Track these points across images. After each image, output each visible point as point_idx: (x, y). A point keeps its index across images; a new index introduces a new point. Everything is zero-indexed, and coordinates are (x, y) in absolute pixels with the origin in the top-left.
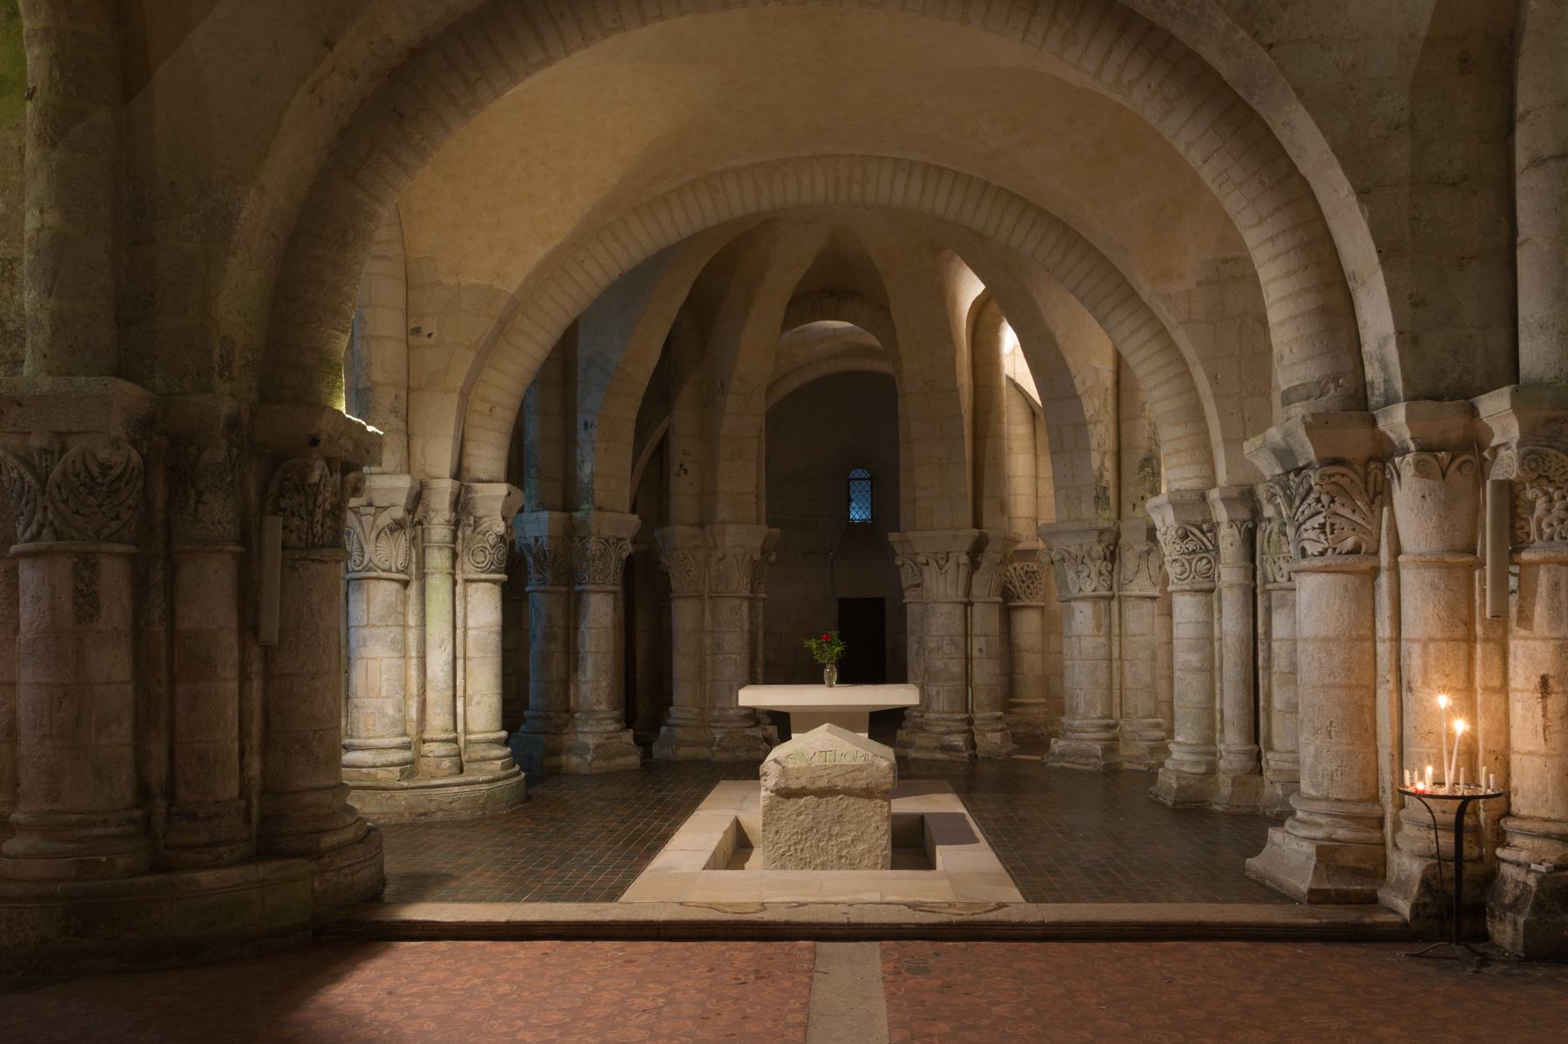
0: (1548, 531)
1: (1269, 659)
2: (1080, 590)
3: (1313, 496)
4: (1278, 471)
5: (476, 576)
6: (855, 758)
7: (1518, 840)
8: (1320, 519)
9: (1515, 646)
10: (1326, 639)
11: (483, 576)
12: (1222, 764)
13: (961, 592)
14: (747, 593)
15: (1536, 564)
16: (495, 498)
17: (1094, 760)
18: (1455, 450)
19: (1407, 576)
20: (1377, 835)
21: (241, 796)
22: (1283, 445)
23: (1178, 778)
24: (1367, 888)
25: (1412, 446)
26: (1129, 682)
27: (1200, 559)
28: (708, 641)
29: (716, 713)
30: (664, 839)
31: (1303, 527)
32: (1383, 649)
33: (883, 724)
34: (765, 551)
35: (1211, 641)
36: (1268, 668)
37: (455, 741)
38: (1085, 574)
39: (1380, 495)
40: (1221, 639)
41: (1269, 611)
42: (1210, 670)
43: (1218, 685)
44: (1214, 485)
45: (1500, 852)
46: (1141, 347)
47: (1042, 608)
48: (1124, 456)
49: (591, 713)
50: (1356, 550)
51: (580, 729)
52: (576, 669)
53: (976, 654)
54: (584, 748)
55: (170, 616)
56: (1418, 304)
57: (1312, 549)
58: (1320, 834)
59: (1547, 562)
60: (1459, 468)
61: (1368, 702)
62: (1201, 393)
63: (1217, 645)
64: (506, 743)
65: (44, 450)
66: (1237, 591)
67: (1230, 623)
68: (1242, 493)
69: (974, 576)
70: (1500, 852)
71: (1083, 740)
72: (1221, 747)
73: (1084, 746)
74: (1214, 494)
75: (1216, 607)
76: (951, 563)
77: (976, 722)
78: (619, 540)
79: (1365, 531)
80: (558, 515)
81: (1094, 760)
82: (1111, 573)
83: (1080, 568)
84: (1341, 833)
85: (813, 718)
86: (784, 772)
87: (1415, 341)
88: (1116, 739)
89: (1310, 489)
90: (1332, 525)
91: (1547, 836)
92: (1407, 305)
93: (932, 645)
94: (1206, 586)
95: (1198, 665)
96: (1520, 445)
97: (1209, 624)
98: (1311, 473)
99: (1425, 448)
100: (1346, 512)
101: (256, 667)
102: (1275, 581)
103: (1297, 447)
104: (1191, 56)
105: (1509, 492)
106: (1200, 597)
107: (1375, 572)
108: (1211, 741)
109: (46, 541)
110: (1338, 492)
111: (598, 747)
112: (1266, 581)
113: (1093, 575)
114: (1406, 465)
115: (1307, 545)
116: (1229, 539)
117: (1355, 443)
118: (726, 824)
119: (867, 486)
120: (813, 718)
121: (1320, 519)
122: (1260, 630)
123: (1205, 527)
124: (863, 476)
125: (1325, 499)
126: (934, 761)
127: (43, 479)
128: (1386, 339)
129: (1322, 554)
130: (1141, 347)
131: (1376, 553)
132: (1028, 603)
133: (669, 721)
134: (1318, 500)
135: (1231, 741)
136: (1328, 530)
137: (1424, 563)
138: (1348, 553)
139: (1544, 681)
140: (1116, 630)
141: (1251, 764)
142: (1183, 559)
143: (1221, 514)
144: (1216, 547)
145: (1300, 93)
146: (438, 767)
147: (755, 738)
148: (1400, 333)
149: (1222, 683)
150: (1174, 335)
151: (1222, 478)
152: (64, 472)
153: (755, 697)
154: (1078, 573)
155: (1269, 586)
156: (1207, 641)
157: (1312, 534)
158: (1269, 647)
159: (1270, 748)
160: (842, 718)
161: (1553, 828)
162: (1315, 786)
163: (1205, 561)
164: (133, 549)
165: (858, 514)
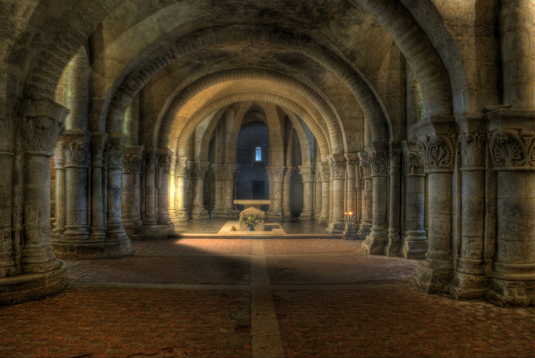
5: (179, 176)
6: (257, 212)
7: (362, 222)
8: (336, 171)
11: (181, 176)
13: (281, 180)
14: (233, 180)
15: (364, 179)
16: (184, 160)
18: (355, 161)
20: (343, 223)
21: (155, 214)
23: (322, 219)
24: (341, 231)
28: (224, 191)
29: (225, 207)
30: (220, 228)
32: (345, 192)
33: (264, 208)
34: (237, 170)
37: (175, 209)
38: (308, 177)
39: (345, 167)
46: (316, 132)
49: (198, 206)
50: (341, 176)
52: (195, 196)
53: (284, 194)
54: (197, 214)
55: (146, 184)
56: (350, 137)
57: (335, 176)
58: (335, 223)
59: (366, 179)
60: (355, 164)
64: (184, 210)
65: (129, 157)
69: (285, 177)
76: (279, 174)
77: (284, 210)
78: (205, 167)
79: (342, 173)
80: (192, 162)
82: (313, 177)
83: (307, 175)
84: (338, 223)
85: (249, 206)
86: (244, 215)
87: (349, 143)
88: (314, 213)
91: (365, 221)
93: (275, 192)
94: (328, 180)
96: (362, 161)
97: (328, 188)
99: (351, 160)
100: (340, 170)
101: (157, 193)
104: (316, 93)
105: (361, 168)
106: (327, 183)
108: (328, 211)
109: (129, 171)
110: (339, 166)
111: (200, 213)
113: (310, 177)
117: (341, 159)
118: (232, 226)
119: (260, 151)
120: (249, 206)
121: (336, 171)
123: (328, 169)
124: (259, 149)
125: (337, 168)
126: (274, 218)
127: (128, 161)
129: (337, 177)
130: (316, 132)
133: (215, 209)
139: (366, 197)
140: (314, 189)
145: (332, 102)
146: (173, 214)
147: (234, 213)
152: (132, 160)
153: (236, 202)
154: (306, 177)
160: (255, 206)
161: (366, 220)
162: (335, 215)
164: (139, 172)
165: (258, 158)
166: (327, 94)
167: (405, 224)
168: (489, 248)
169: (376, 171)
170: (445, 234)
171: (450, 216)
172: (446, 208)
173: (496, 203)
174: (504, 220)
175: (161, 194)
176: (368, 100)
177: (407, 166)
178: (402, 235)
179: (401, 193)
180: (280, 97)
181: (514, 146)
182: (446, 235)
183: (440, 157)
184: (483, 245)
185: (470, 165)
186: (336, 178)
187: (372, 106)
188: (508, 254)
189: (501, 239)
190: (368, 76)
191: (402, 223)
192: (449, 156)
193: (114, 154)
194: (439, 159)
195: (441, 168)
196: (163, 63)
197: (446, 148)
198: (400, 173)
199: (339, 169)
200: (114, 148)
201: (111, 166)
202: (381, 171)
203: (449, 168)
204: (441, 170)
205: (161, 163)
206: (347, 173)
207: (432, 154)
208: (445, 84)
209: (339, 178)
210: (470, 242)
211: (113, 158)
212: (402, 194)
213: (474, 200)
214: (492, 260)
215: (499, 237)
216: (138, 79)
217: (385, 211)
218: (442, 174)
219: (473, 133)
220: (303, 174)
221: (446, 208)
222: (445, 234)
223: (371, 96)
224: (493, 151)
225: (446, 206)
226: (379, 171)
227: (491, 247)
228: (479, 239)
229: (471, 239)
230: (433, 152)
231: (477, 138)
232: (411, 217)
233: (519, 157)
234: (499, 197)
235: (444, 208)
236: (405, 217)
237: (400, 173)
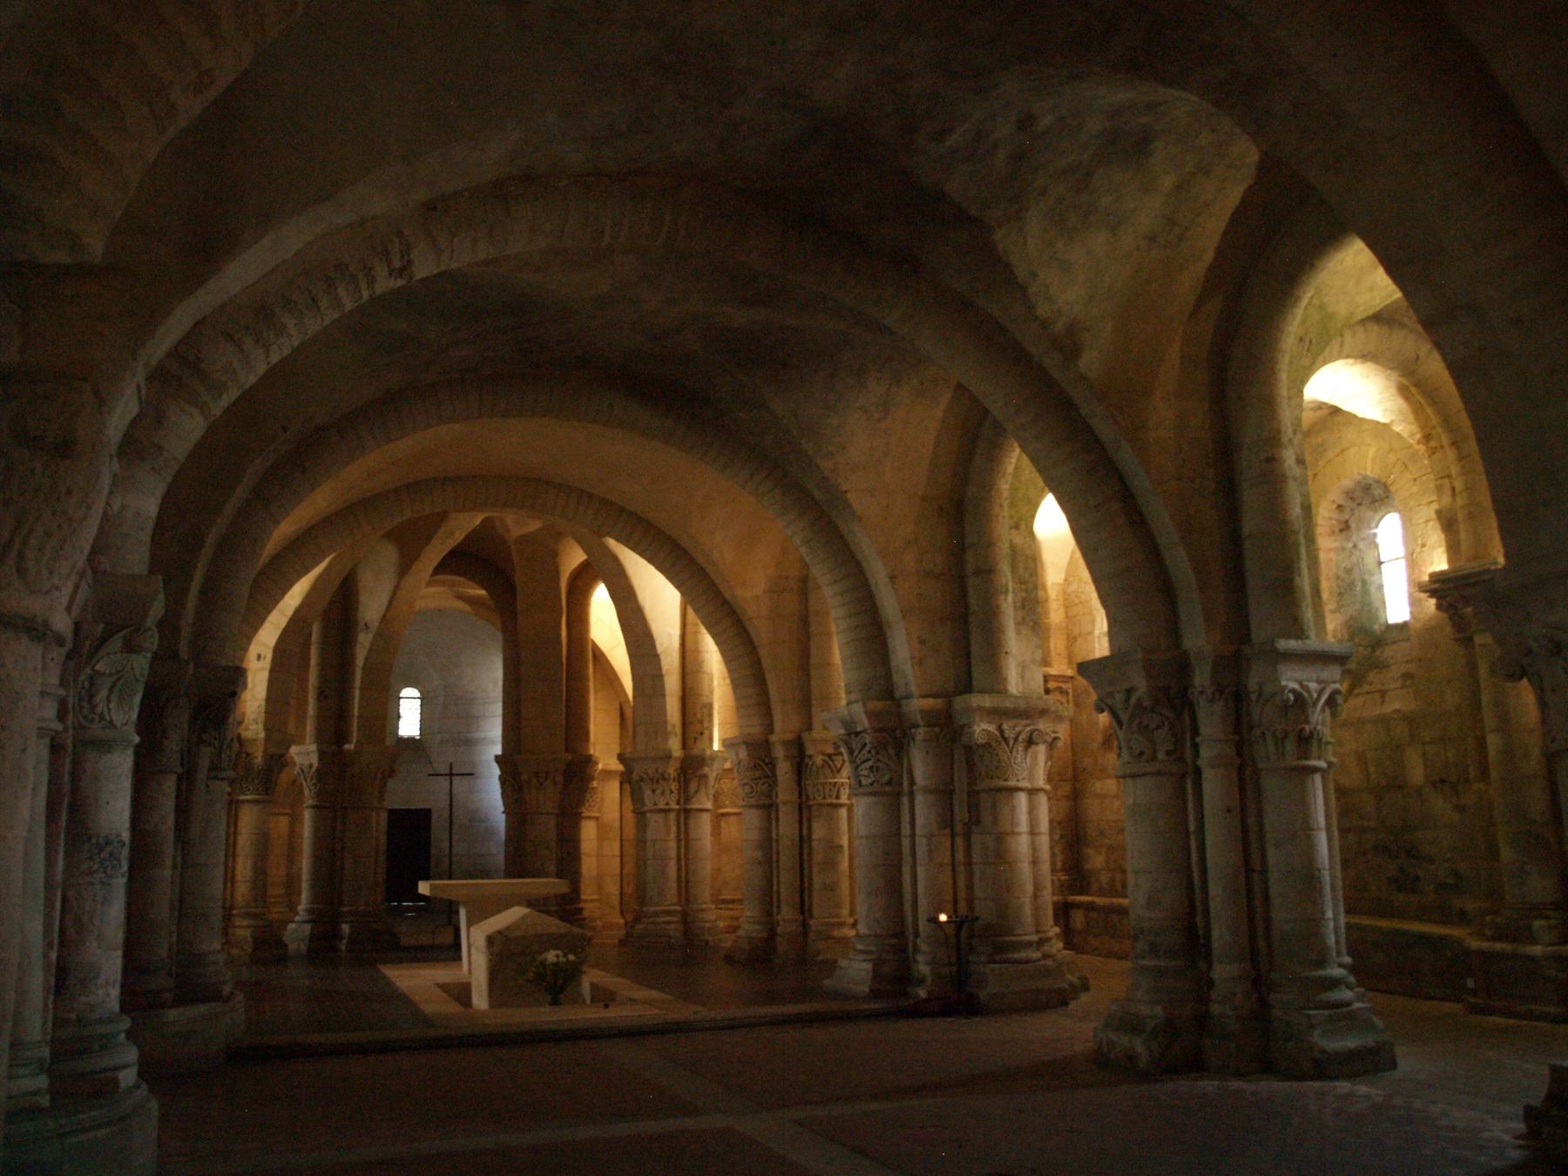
1: (810, 854)
2: (655, 804)
8: (868, 765)
12: (779, 929)
19: (919, 798)
25: (921, 722)
27: (764, 784)
31: (860, 768)
32: (906, 842)
36: (810, 859)
40: (777, 841)
41: (809, 820)
43: (775, 873)
50: (889, 783)
51: (237, 923)
63: (774, 844)
67: (786, 827)
71: (659, 923)
72: (779, 917)
75: (773, 816)
83: (655, 786)
89: (864, 745)
90: (877, 767)
98: (866, 736)
102: (814, 799)
107: (899, 794)
108: (769, 914)
112: (808, 799)
114: (920, 733)
115: (862, 779)
116: (784, 769)
121: (868, 765)
123: (767, 761)
125: (873, 752)
129: (871, 784)
131: (901, 784)
132: (589, 814)
134: (869, 752)
135: (787, 914)
136: (874, 770)
137: (928, 791)
138: (886, 784)
141: (800, 929)
143: (779, 752)
144: (774, 775)
149: (779, 872)
151: (778, 726)
154: (653, 791)
155: (811, 803)
157: (865, 773)
158: (810, 845)
159: (811, 916)
163: (767, 785)
169: (1141, 753)
186: (870, 789)
193: (111, 675)
196: (357, 289)
199: (880, 757)
200: (116, 643)
201: (96, 730)
202: (1161, 756)
211: (104, 693)
216: (249, 342)
226: (1155, 752)
236: (1267, 919)
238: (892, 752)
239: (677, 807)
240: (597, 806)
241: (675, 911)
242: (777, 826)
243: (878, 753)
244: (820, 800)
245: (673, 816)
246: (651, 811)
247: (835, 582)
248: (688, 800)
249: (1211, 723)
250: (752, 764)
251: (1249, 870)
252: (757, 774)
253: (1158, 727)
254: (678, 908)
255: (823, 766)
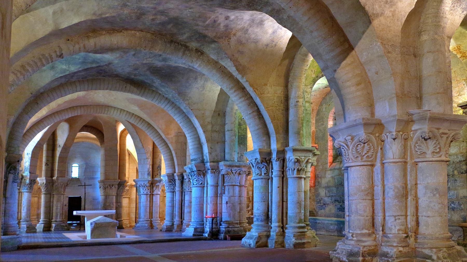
0: (228, 181)
1: (184, 204)
3: (195, 175)
4: (190, 171)
8: (196, 179)
9: (223, 197)
10: (196, 197)
12: (175, 223)
17: (145, 227)
19: (209, 188)
20: (203, 226)
22: (191, 167)
24: (202, 234)
26: (153, 212)
32: (205, 199)
35: (173, 201)
36: (184, 206)
38: (145, 189)
41: (184, 195)
42: (173, 206)
44: (175, 173)
45: (220, 227)
47: (129, 198)
48: (154, 165)
50: (201, 184)
56: (211, 148)
61: (202, 206)
62: (173, 155)
63: (174, 202)
66: (179, 192)
67: (177, 197)
68: (181, 174)
70: (220, 227)
73: (143, 224)
74: (175, 174)
75: (175, 195)
81: (145, 227)
83: (144, 188)
84: (198, 226)
89: (195, 174)
92: (210, 148)
94: (173, 191)
95: (171, 205)
100: (200, 178)
103: (193, 168)
112: (184, 190)
114: (209, 172)
116: (178, 183)
121: (196, 179)
122: (183, 199)
123: (173, 180)
125: (197, 176)
128: (207, 153)
129: (196, 184)
131: (204, 184)
134: (196, 176)
135: (177, 220)
137: (211, 186)
139: (227, 202)
141: (180, 223)
142: (169, 186)
143: (177, 178)
148: (209, 152)
150: (169, 145)
151: (177, 171)
154: (143, 189)
155: (185, 191)
156: (173, 200)
157: (195, 181)
158: (184, 202)
159: (184, 220)
166: (192, 109)
167: (287, 219)
168: (411, 223)
169: (258, 174)
170: (368, 216)
171: (371, 201)
172: (369, 194)
173: (416, 188)
174: (425, 201)
175: (8, 203)
176: (253, 112)
177: (289, 169)
178: (284, 229)
179: (283, 192)
180: (127, 111)
181: (435, 141)
182: (369, 217)
183: (365, 152)
184: (406, 222)
185: (395, 158)
187: (256, 117)
188: (430, 227)
189: (422, 216)
190: (256, 90)
191: (285, 219)
192: (373, 151)
194: (364, 154)
195: (365, 161)
197: (371, 144)
198: (282, 175)
202: (263, 174)
203: (371, 161)
204: (366, 163)
205: (10, 170)
206: (207, 180)
207: (357, 149)
208: (368, 93)
209: (199, 185)
210: (396, 220)
212: (284, 194)
213: (399, 186)
214: (414, 234)
215: (419, 214)
217: (267, 209)
218: (364, 167)
219: (399, 132)
220: (140, 186)
221: (369, 194)
222: (368, 216)
223: (256, 108)
224: (415, 146)
225: (369, 193)
227: (414, 223)
228: (403, 217)
229: (397, 218)
230: (358, 148)
231: (402, 135)
232: (294, 213)
233: (438, 150)
234: (418, 182)
235: (367, 195)
236: (287, 213)
237: (282, 175)
238: (202, 176)
239: (150, 193)
240: (129, 194)
241: (148, 220)
242: (175, 197)
243: (198, 176)
244: (187, 190)
245: (148, 195)
246: (142, 194)
247: (189, 133)
248: (153, 192)
249: (276, 166)
250: (169, 181)
251: (283, 201)
252: (170, 184)
253: (263, 168)
254: (150, 219)
255: (188, 182)
